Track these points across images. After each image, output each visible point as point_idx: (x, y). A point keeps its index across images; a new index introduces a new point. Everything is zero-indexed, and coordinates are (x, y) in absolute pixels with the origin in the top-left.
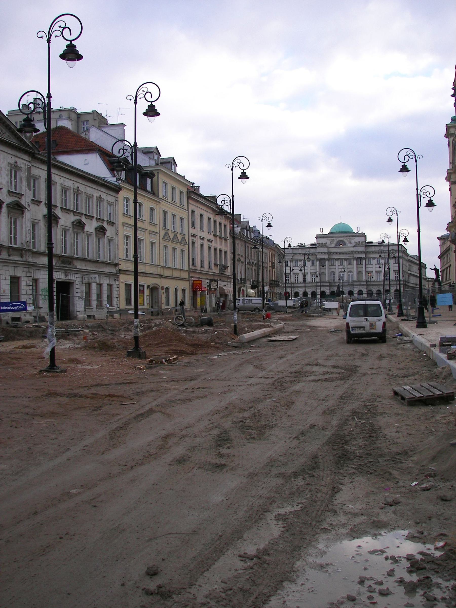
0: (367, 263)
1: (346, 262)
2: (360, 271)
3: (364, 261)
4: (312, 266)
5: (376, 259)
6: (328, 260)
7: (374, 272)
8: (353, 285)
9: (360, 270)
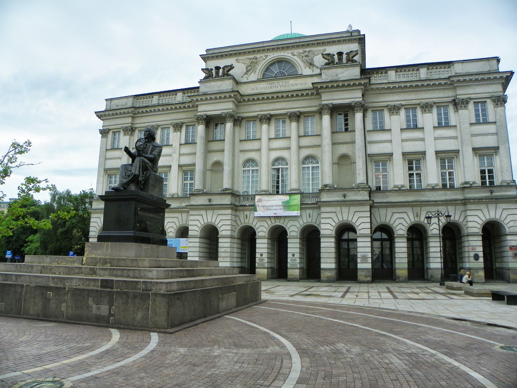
0: (369, 126)
1: (294, 124)
2: (344, 157)
3: (359, 116)
4: (186, 143)
5: (403, 112)
6: (237, 121)
7: (398, 158)
8: (318, 205)
9: (343, 150)
